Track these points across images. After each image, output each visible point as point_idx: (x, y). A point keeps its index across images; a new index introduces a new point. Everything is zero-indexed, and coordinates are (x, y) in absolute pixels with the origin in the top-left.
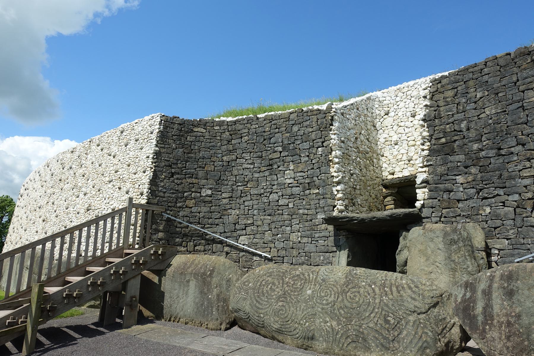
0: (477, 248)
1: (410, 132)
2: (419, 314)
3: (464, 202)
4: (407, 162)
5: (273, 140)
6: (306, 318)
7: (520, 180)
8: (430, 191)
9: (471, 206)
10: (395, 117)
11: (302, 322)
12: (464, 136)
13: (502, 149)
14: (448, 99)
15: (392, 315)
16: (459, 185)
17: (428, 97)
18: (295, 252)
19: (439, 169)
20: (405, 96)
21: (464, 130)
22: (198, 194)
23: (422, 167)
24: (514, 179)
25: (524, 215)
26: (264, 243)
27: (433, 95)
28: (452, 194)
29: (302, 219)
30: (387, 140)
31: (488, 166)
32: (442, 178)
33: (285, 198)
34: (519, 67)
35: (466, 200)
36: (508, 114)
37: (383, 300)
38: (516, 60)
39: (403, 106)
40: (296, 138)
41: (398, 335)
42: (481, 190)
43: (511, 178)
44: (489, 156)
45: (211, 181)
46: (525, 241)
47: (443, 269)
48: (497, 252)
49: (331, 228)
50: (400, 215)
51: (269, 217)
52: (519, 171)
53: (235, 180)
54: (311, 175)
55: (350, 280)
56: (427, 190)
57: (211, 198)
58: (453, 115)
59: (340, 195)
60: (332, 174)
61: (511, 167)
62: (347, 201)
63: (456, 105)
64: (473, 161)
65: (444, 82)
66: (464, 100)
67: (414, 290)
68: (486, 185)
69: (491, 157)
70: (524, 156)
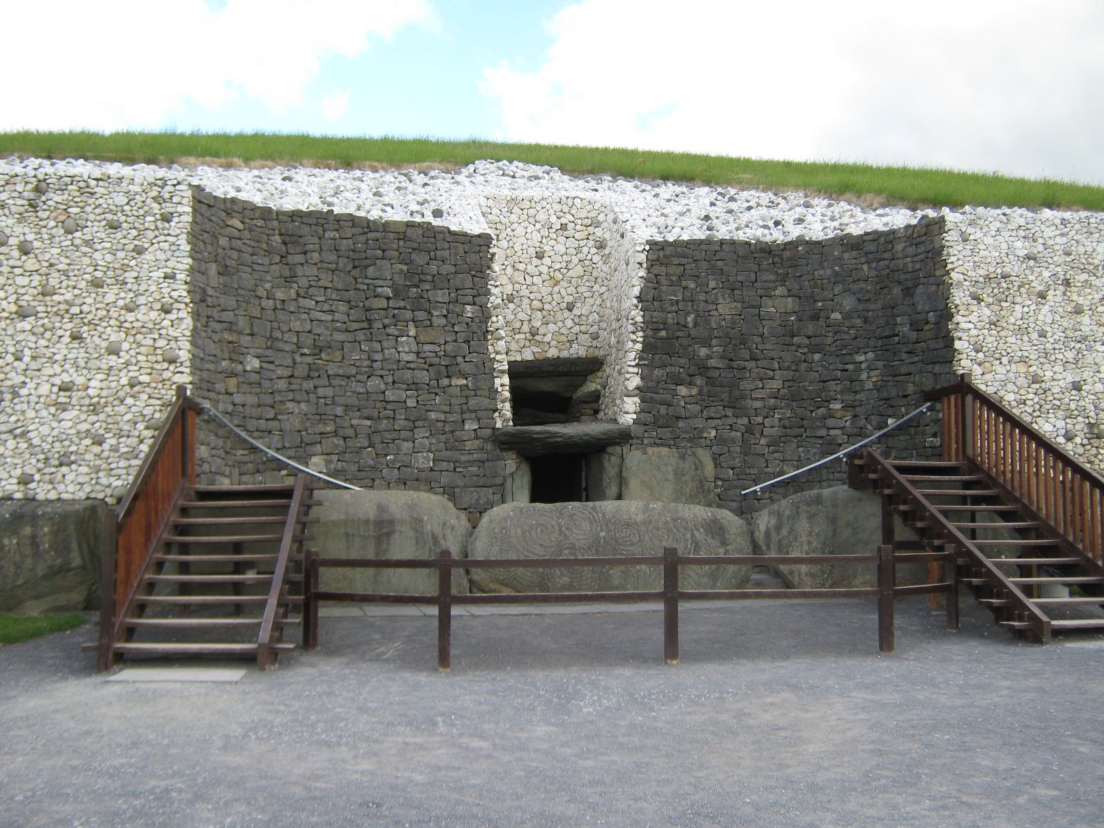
4: (529, 337)
5: (371, 270)
10: (508, 251)
19: (656, 372)
21: (691, 325)
22: (240, 367)
24: (745, 399)
26: (359, 471)
32: (660, 386)
33: (398, 389)
38: (757, 255)
40: (422, 277)
45: (260, 341)
49: (489, 446)
51: (368, 423)
53: (295, 340)
57: (257, 376)
58: (677, 302)
60: (492, 356)
61: (744, 385)
65: (668, 251)
66: (692, 286)
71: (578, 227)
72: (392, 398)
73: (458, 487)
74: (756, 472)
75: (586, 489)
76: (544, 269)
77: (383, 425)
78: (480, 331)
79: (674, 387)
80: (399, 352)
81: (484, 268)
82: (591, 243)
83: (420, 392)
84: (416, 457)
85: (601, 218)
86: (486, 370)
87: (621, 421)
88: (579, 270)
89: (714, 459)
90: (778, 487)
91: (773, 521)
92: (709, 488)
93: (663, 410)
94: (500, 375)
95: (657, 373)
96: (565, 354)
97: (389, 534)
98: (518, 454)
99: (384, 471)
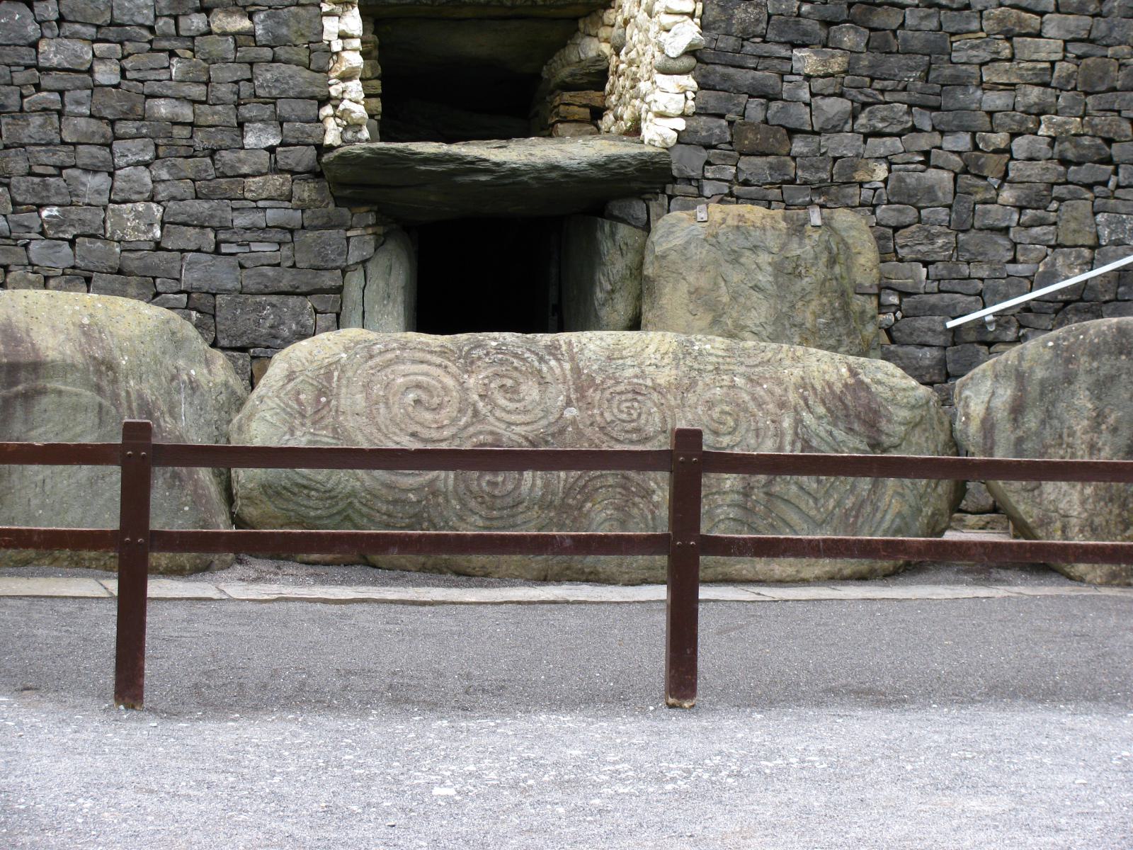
0: (861, 285)
3: (810, 138)
6: (585, 486)
7: (979, 93)
8: (702, 86)
11: (570, 501)
16: (798, 78)
24: (965, 85)
25: (978, 197)
28: (775, 106)
29: (166, 143)
32: (749, 47)
33: (74, 36)
35: (818, 133)
37: (802, 421)
41: (834, 508)
42: (865, 105)
43: (960, 82)
48: (894, 299)
49: (305, 191)
50: (630, 164)
52: (981, 65)
55: (691, 368)
56: (696, 85)
67: (873, 390)
68: (882, 91)
69: (903, 7)
70: (1000, 21)
72: (55, 61)
73: (228, 292)
74: (984, 274)
75: (558, 309)
77: (32, 130)
83: (130, 47)
84: (119, 215)
89: (878, 238)
90: (1039, 313)
91: (1006, 393)
92: (863, 312)
93: (755, 110)
94: (338, 9)
97: (29, 397)
99: (33, 247)
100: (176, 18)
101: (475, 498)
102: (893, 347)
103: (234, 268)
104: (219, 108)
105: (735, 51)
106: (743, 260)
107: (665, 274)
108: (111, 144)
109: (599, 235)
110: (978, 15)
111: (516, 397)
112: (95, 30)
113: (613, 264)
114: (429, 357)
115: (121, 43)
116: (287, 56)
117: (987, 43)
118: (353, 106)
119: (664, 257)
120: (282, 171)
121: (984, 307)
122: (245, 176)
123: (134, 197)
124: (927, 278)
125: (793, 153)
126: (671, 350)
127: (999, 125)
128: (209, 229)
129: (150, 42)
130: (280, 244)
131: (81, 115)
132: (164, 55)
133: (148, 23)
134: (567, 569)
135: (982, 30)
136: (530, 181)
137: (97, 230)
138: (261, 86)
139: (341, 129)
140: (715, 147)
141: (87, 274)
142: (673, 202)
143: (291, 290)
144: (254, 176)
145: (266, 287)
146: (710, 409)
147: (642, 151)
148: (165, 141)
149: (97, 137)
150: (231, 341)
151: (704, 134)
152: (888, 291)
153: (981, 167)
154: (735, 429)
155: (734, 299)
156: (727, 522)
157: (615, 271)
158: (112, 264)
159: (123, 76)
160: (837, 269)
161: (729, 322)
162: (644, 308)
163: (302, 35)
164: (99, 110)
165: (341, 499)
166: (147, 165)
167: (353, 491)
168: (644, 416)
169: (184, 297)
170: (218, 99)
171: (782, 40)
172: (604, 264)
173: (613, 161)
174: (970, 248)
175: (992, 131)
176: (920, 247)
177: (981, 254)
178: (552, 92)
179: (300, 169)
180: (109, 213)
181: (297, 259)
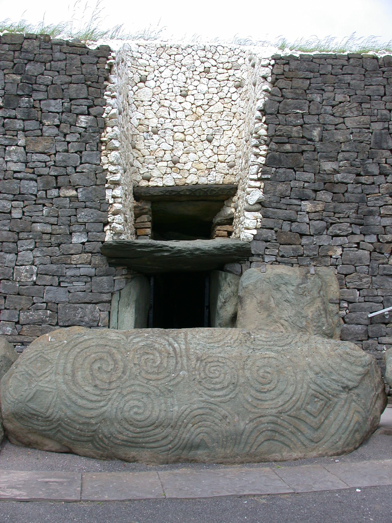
1: (177, 118)
2: (350, 390)
6: (188, 414)
7: (379, 218)
8: (264, 217)
9: (318, 244)
10: (155, 90)
11: (180, 423)
12: (315, 148)
13: (362, 176)
14: (297, 91)
15: (320, 395)
17: (269, 79)
18: (24, 302)
20: (173, 61)
21: (317, 139)
23: (255, 180)
25: (381, 261)
27: (277, 79)
28: (294, 225)
29: (39, 241)
30: (141, 123)
31: (343, 194)
32: (283, 201)
34: (388, 79)
36: (372, 133)
38: (385, 69)
39: (170, 75)
40: (35, 87)
41: (324, 420)
42: (332, 224)
44: (345, 181)
46: (379, 292)
47: (290, 329)
48: (346, 305)
49: (97, 260)
52: (380, 207)
54: (64, 161)
59: (117, 206)
60: (105, 167)
62: (123, 215)
63: (308, 102)
64: (325, 184)
65: (293, 64)
66: (319, 99)
68: (339, 218)
69: (347, 184)
70: (387, 189)
71: (220, 71)
73: (63, 302)
75: (208, 307)
76: (187, 106)
78: (93, 140)
79: (299, 203)
80: (7, 162)
81: (101, 79)
82: (231, 84)
83: (26, 203)
84: (18, 270)
85: (241, 61)
86: (99, 179)
87: (242, 237)
88: (219, 106)
93: (286, 226)
94: (112, 186)
95: (281, 187)
96: (203, 181)
98: (129, 269)
100: (46, 191)
101: (127, 422)
102: (345, 325)
103: (66, 292)
104: (62, 227)
105: (277, 202)
106: (280, 289)
107: (247, 295)
108: (17, 242)
109: (220, 278)
110: (378, 187)
111: (154, 365)
112: (13, 196)
113: (225, 290)
114: (110, 343)
115: (23, 201)
116: (91, 205)
117: (382, 198)
118: (118, 226)
119: (246, 288)
120: (88, 252)
121: (384, 309)
122: (72, 254)
123: (26, 263)
124: (359, 296)
125: (302, 244)
126: (239, 338)
127: (388, 232)
128: (55, 277)
129: (35, 201)
130: (86, 282)
131: (6, 230)
132: (41, 206)
133: (34, 193)
134: (179, 458)
135: (380, 193)
136: (187, 255)
137: (9, 277)
138: (80, 218)
139: (112, 235)
140: (269, 241)
141: (5, 295)
142: (252, 264)
143: (89, 302)
144: (76, 255)
145: (79, 300)
146: (258, 371)
147: (238, 243)
148: (39, 240)
149: (11, 239)
150: (64, 323)
151: (265, 236)
152: (343, 301)
153: (380, 249)
154: (271, 381)
155: (277, 305)
156: (267, 431)
157: (226, 294)
158: (15, 291)
159: (23, 215)
160: (321, 293)
161: (275, 316)
162: (239, 309)
163: (97, 197)
164: (13, 228)
165: (55, 422)
166: (32, 250)
167: (60, 417)
168: (222, 375)
169: (45, 305)
170: (62, 223)
171: (297, 198)
172: (221, 290)
173: (224, 247)
174: (377, 283)
175: (385, 234)
176: (356, 283)
177: (382, 286)
178: (215, 227)
179: (95, 251)
180: (15, 270)
181: (93, 289)
